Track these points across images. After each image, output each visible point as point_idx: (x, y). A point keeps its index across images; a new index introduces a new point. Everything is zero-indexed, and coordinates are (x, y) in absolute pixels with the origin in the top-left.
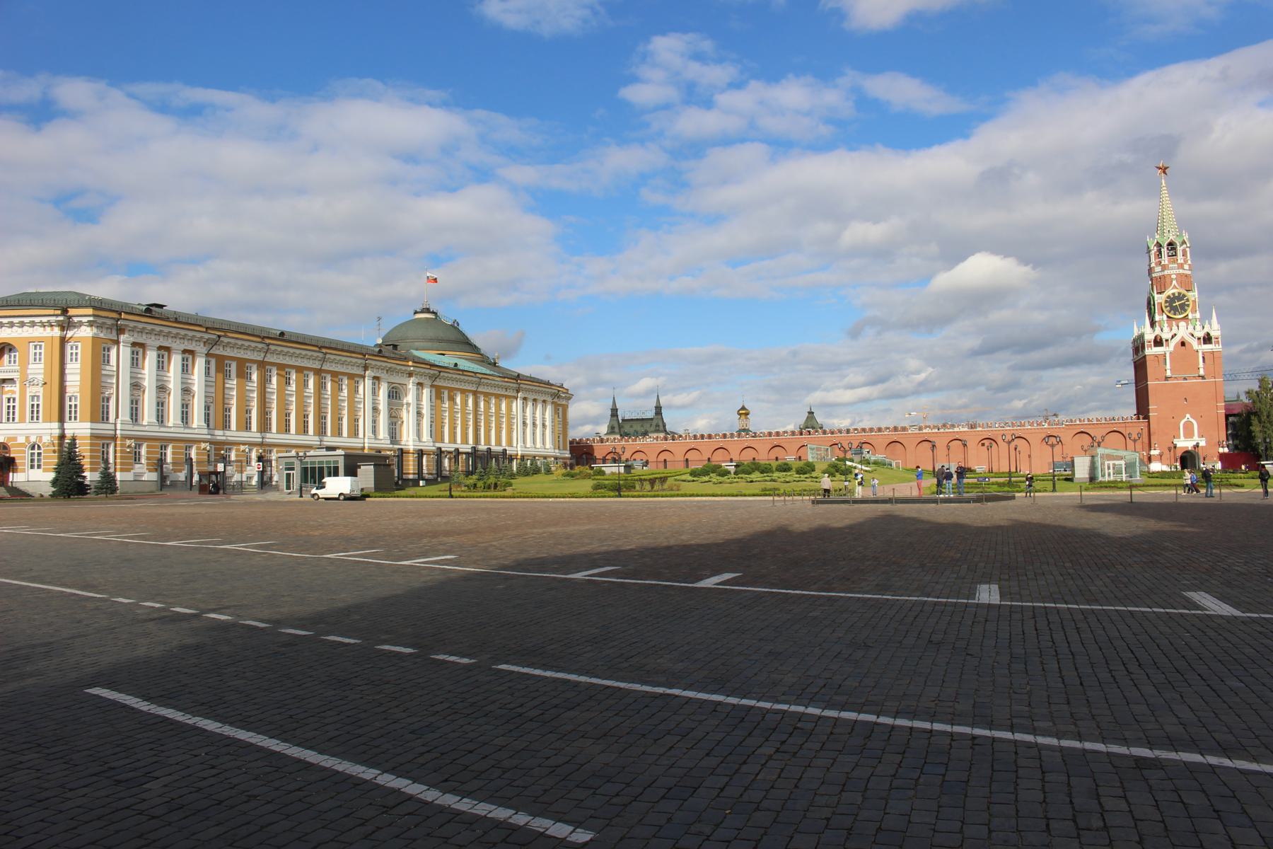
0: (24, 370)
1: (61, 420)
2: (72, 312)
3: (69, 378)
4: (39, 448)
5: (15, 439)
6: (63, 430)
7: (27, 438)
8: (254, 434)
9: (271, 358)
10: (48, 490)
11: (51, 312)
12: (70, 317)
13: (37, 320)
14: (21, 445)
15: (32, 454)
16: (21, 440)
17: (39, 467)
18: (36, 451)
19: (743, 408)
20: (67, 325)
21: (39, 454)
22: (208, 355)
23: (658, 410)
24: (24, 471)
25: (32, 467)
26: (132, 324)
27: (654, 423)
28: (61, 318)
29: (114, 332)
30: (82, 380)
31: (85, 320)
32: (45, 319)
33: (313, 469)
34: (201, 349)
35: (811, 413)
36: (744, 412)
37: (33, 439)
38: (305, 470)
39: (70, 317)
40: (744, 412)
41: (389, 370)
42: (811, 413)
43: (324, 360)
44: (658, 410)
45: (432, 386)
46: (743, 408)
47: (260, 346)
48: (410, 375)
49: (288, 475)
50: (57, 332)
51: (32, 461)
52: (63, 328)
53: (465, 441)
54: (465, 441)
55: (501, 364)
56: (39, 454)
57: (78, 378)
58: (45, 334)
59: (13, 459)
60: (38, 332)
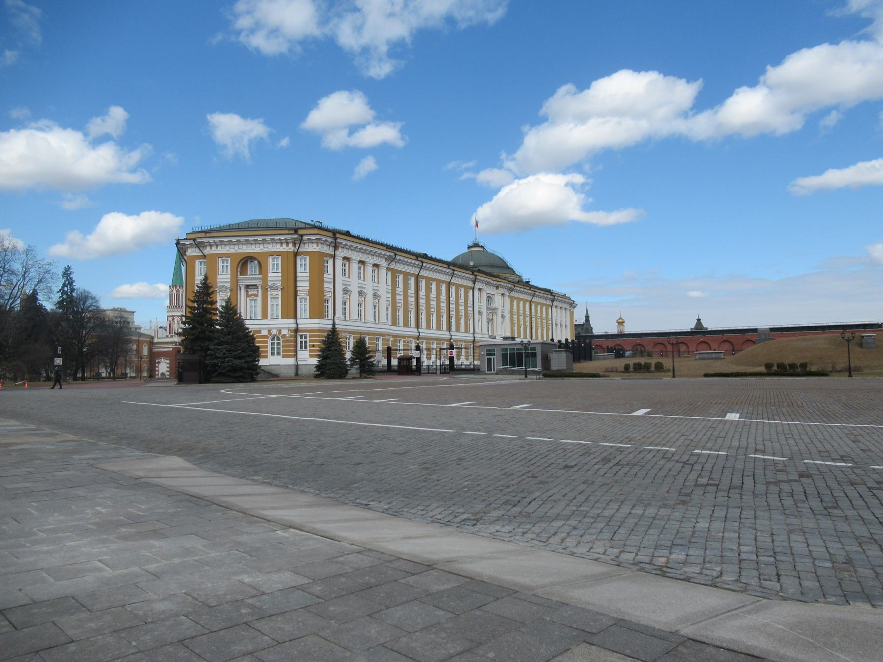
0: (265, 279)
1: (296, 318)
2: (301, 232)
3: (299, 284)
4: (278, 339)
5: (260, 332)
6: (297, 324)
7: (269, 331)
8: (412, 331)
9: (423, 273)
10: (313, 370)
11: (287, 232)
12: (302, 236)
13: (276, 238)
15: (273, 344)
16: (264, 332)
17: (278, 354)
19: (621, 318)
20: (301, 241)
21: (278, 344)
22: (388, 269)
23: (587, 317)
24: (266, 357)
25: (273, 354)
26: (344, 242)
27: (585, 327)
28: (296, 236)
29: (332, 249)
30: (310, 286)
31: (313, 238)
32: (282, 237)
33: (512, 355)
34: (383, 263)
35: (699, 320)
36: (621, 323)
37: (274, 332)
38: (504, 356)
39: (302, 236)
40: (621, 323)
41: (488, 284)
42: (699, 320)
43: (453, 275)
44: (587, 317)
45: (509, 297)
46: (621, 318)
47: (418, 263)
48: (497, 288)
49: (489, 360)
51: (273, 349)
52: (294, 244)
53: (525, 337)
54: (525, 337)
55: (532, 283)
56: (278, 344)
57: (307, 284)
58: (281, 249)
59: (258, 347)
60: (277, 248)
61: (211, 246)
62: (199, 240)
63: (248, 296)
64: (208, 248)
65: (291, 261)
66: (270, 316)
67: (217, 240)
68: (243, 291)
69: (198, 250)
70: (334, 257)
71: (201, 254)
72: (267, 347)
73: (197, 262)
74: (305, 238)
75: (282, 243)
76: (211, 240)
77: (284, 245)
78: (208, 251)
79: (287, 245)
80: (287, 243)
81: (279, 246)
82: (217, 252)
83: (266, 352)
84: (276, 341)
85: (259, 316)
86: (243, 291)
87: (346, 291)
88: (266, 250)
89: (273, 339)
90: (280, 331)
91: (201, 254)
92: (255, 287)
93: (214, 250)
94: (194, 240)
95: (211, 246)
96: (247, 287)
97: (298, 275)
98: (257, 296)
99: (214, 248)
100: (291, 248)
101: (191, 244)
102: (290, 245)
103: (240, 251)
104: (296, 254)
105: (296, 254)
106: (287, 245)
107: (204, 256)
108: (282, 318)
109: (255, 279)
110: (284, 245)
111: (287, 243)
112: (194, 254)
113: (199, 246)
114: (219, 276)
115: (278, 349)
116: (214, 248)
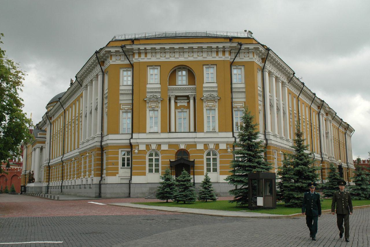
3: (234, 95)
5: (195, 145)
7: (206, 145)
12: (241, 45)
13: (214, 46)
14: (201, 151)
15: (209, 160)
16: (200, 147)
17: (215, 170)
18: (211, 157)
32: (221, 46)
37: (212, 146)
39: (241, 45)
50: (228, 57)
51: (208, 165)
52: (230, 53)
58: (217, 59)
61: (140, 54)
62: (128, 47)
63: (176, 107)
64: (136, 56)
65: (225, 72)
66: (206, 130)
67: (148, 47)
68: (173, 102)
69: (123, 58)
70: (263, 70)
71: (127, 62)
72: (202, 162)
73: (121, 71)
74: (243, 47)
75: (217, 52)
76: (142, 47)
77: (220, 54)
78: (136, 59)
79: (224, 54)
80: (224, 52)
81: (214, 54)
82: (146, 60)
83: (202, 168)
84: (211, 157)
85: (192, 129)
86: (173, 102)
87: (271, 106)
88: (200, 58)
89: (209, 154)
90: (217, 145)
91: (127, 62)
92: (188, 97)
93: (143, 59)
94: (122, 47)
95: (140, 54)
96: (177, 97)
97: (234, 86)
98: (188, 107)
99: (143, 56)
100: (228, 57)
101: (116, 52)
102: (227, 54)
103: (172, 59)
104: (232, 64)
105: (232, 64)
106: (224, 54)
107: (132, 66)
108: (220, 131)
109: (185, 89)
110: (220, 54)
111: (224, 52)
112: (119, 62)
113: (127, 53)
114: (148, 86)
115: (215, 165)
116: (143, 56)
